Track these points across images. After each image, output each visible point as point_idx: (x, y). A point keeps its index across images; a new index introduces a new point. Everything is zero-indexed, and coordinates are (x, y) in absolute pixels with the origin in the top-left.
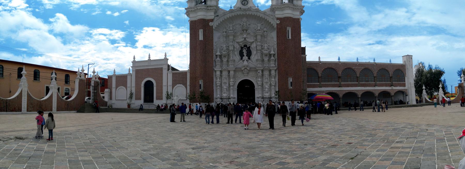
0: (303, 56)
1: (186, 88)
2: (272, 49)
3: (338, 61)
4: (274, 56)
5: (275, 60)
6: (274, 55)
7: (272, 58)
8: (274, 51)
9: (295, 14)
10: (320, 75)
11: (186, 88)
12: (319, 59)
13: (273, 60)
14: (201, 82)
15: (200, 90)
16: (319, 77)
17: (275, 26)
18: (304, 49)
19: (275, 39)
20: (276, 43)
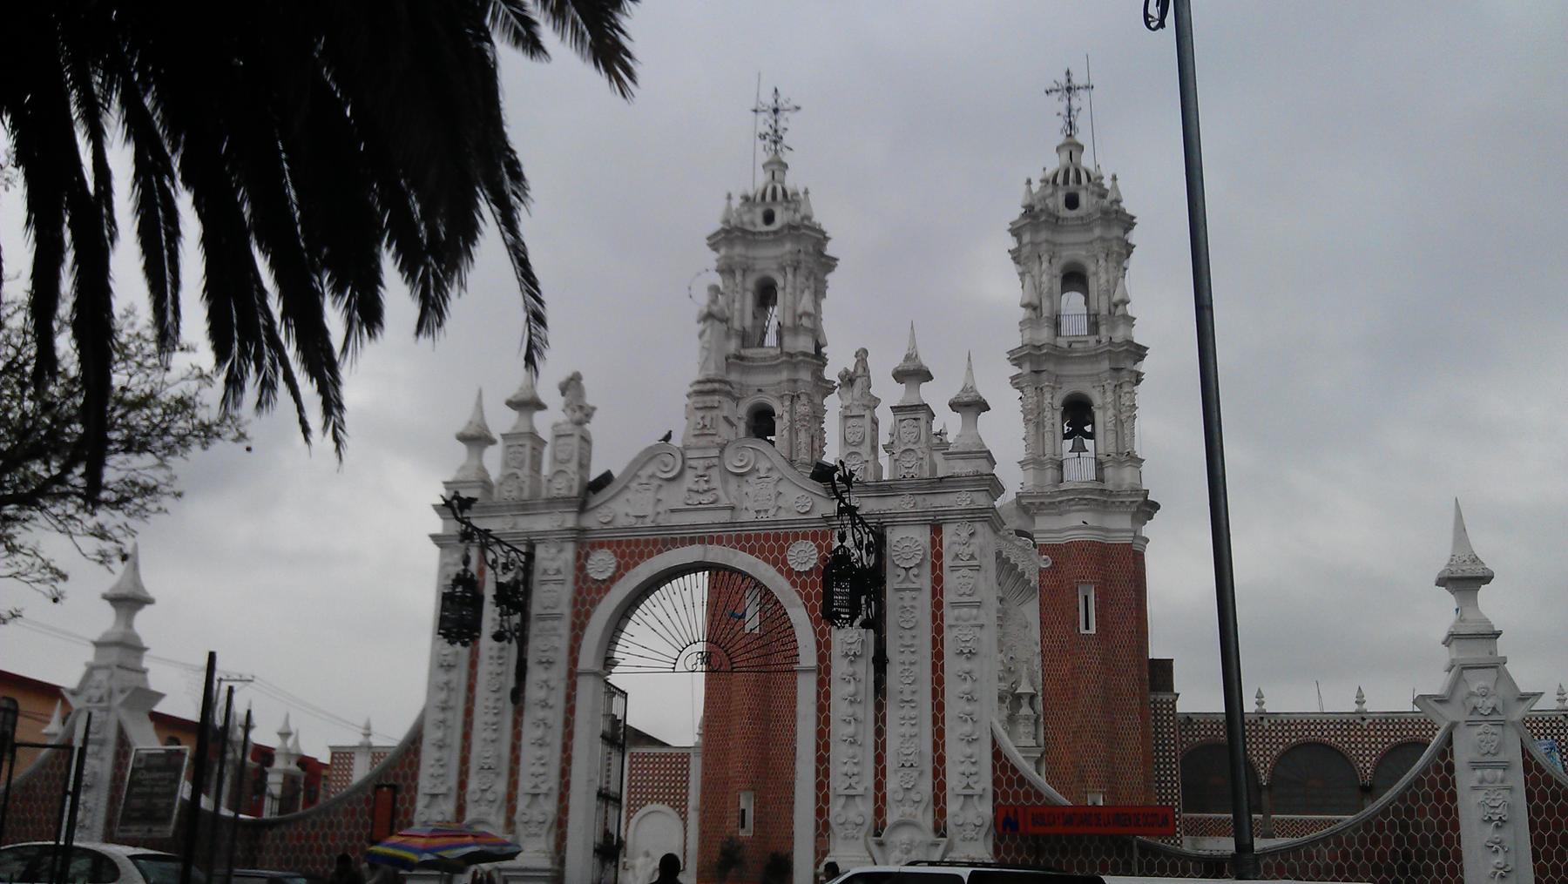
0: (1165, 697)
1: (685, 820)
2: (1024, 674)
3: (1353, 708)
4: (1031, 704)
5: (1037, 721)
6: (1032, 697)
7: (1025, 710)
8: (1032, 683)
9: (1118, 526)
10: (1264, 779)
11: (685, 820)
12: (1260, 704)
13: (1027, 718)
14: (747, 803)
15: (742, 833)
16: (1260, 788)
17: (1035, 581)
18: (1165, 667)
19: (1036, 633)
20: (1038, 649)
